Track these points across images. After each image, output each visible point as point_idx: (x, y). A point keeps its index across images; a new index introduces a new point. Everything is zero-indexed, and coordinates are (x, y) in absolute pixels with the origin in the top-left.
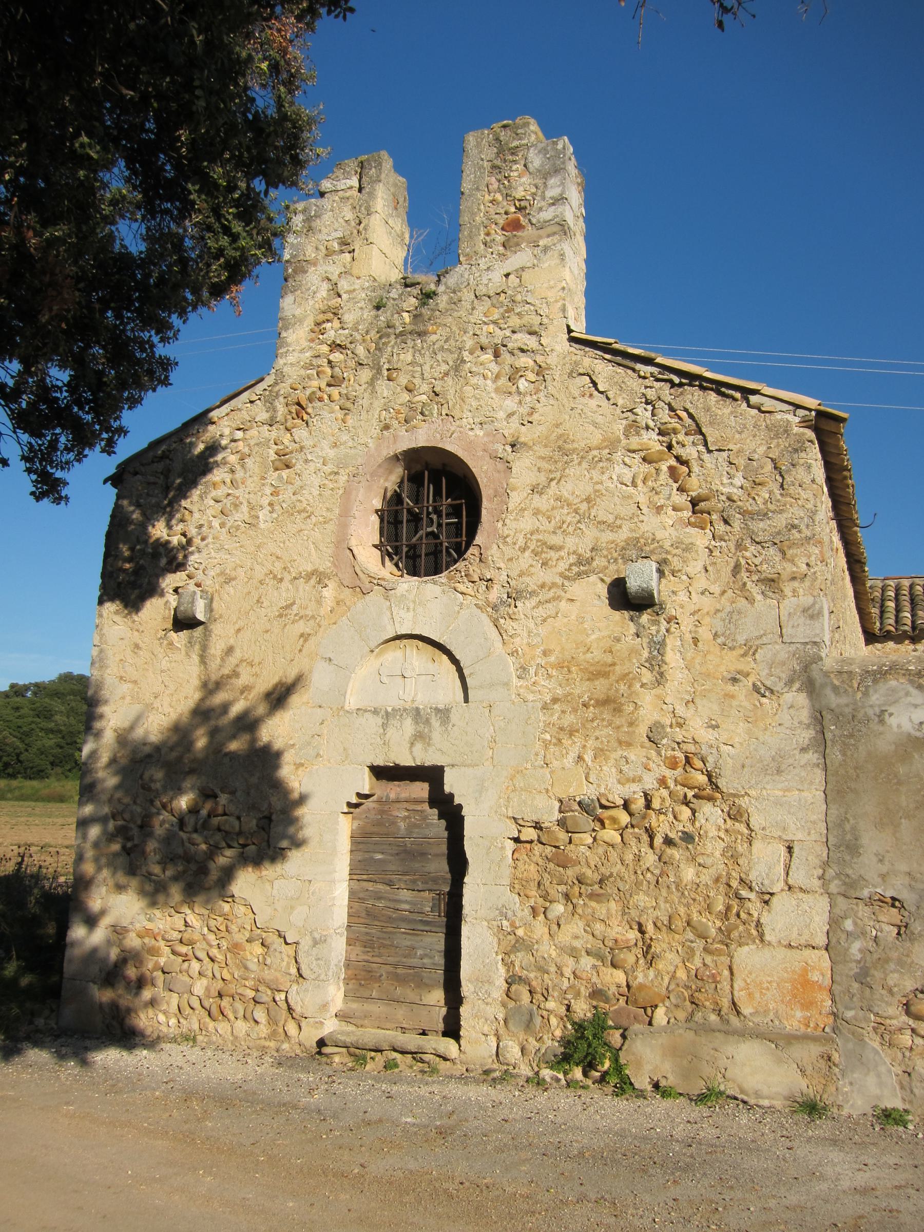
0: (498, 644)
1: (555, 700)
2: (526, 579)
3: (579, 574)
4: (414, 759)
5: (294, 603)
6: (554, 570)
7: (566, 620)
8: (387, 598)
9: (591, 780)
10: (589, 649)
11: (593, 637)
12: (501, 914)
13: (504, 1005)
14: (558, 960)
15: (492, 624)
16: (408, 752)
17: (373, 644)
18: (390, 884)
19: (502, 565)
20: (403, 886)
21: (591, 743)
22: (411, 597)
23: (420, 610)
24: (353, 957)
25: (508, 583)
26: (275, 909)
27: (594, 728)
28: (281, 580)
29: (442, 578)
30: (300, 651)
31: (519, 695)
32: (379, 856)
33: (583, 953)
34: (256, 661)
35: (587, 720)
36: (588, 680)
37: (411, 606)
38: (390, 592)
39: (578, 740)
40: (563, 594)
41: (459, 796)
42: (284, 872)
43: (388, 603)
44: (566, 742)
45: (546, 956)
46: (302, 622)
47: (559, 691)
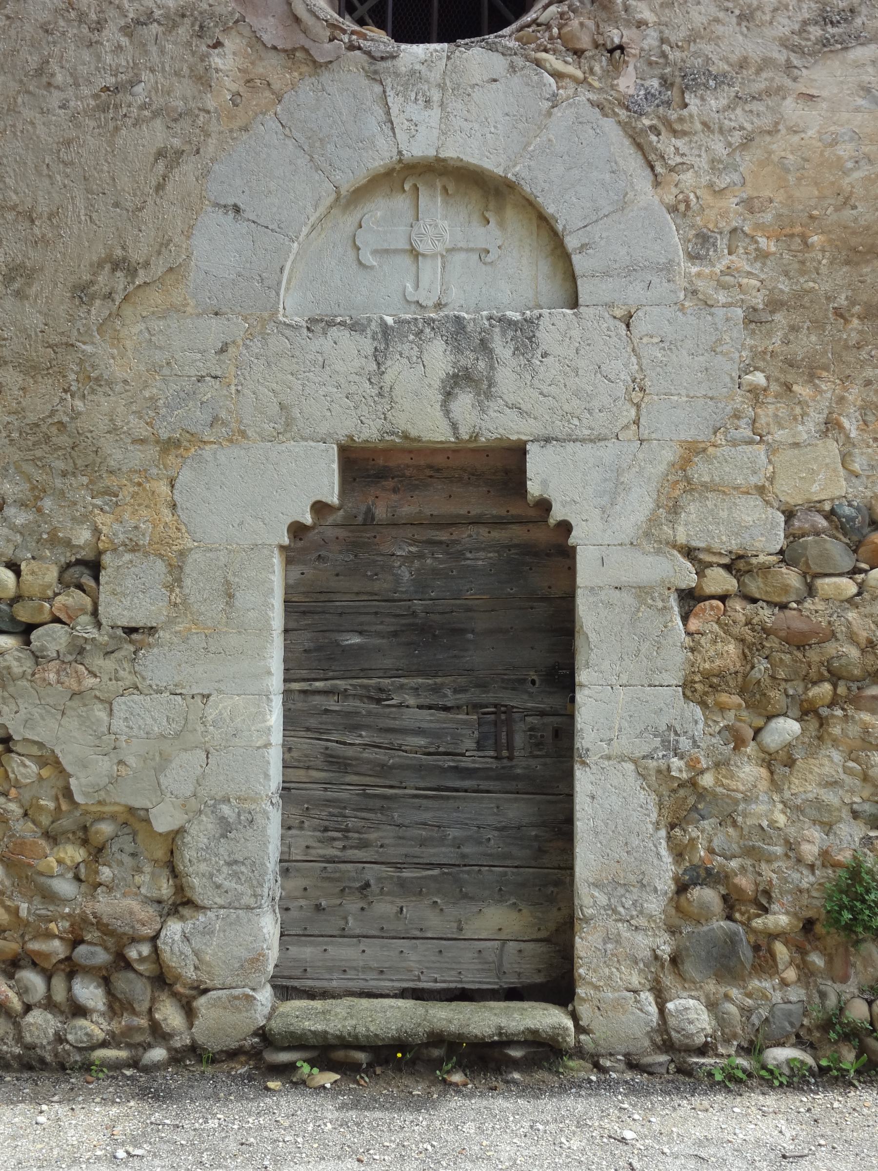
0: (643, 181)
1: (775, 304)
2: (708, 48)
3: (825, 43)
4: (454, 427)
5: (134, 82)
6: (768, 32)
7: (795, 139)
8: (374, 77)
9: (856, 467)
10: (847, 199)
11: (857, 175)
12: (666, 744)
13: (673, 930)
14: (792, 831)
15: (627, 142)
16: (439, 414)
17: (348, 181)
18: (379, 697)
19: (647, 15)
20: (412, 701)
21: (854, 394)
22: (435, 76)
23: (456, 105)
24: (297, 854)
25: (664, 55)
26: (120, 762)
27: (863, 364)
28: (99, 26)
29: (507, 37)
30: (160, 187)
31: (695, 292)
32: (356, 640)
33: (845, 814)
34: (43, 208)
35: (847, 347)
36: (847, 262)
37: (436, 95)
38: (383, 64)
39: (828, 387)
40: (788, 82)
41: (564, 504)
42: (138, 681)
43: (378, 89)
44: (802, 390)
45: (765, 824)
46: (158, 123)
47: (784, 286)
